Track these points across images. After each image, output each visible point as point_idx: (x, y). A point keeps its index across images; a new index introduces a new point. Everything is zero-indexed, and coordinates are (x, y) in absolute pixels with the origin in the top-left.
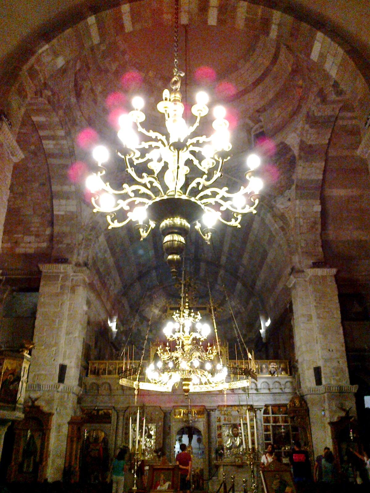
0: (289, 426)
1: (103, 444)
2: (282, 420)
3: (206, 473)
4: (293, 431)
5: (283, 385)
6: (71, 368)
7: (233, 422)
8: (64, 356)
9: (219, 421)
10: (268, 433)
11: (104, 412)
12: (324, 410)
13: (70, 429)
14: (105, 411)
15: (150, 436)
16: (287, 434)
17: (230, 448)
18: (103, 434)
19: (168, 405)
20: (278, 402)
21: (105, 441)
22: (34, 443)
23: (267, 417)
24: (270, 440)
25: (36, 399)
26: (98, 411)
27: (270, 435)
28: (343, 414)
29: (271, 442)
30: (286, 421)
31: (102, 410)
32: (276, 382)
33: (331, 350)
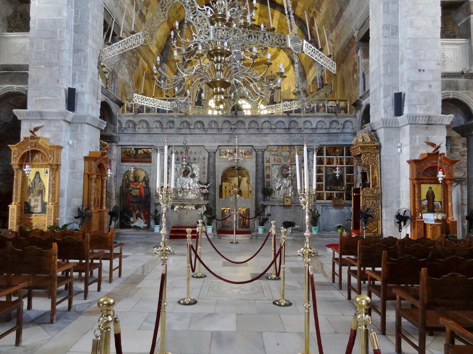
0: (344, 167)
1: (144, 183)
2: (337, 162)
4: (347, 173)
5: (341, 124)
6: (83, 93)
7: (283, 162)
8: (74, 80)
9: (268, 161)
10: (321, 174)
11: (143, 151)
12: (400, 147)
13: (87, 166)
14: (145, 150)
15: (193, 176)
16: (341, 176)
17: (279, 189)
18: (144, 173)
19: (213, 144)
20: (335, 143)
21: (146, 180)
22: (40, 180)
23: (321, 158)
24: (322, 181)
25: (36, 129)
26: (137, 150)
27: (322, 176)
28: (431, 150)
29: (324, 183)
30: (341, 163)
31: (141, 149)
32: (334, 121)
33: (422, 71)
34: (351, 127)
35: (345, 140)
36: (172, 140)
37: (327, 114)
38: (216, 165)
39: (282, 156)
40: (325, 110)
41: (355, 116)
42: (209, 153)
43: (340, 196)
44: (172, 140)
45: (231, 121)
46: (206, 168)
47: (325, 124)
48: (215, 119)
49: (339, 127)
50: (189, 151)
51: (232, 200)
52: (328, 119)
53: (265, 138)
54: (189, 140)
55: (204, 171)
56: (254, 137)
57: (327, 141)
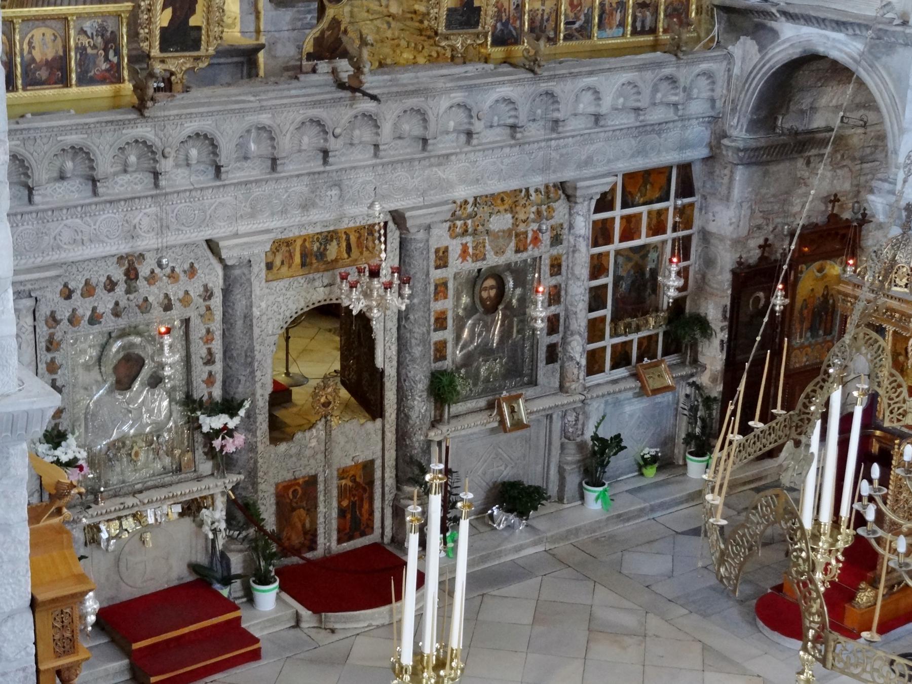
3: (386, 477)
23: (604, 221)
29: (607, 312)
34: (706, 94)
35: (683, 146)
36: (67, 236)
37: (629, 39)
38: (256, 312)
39: (487, 232)
40: (622, 24)
41: (729, 57)
42: (226, 267)
43: (647, 348)
44: (67, 236)
45: (329, 125)
46: (218, 334)
47: (639, 93)
48: (265, 119)
49: (674, 99)
50: (144, 270)
51: (314, 443)
52: (649, 75)
53: (439, 172)
54: (146, 222)
55: (210, 352)
56: (401, 175)
57: (633, 156)
